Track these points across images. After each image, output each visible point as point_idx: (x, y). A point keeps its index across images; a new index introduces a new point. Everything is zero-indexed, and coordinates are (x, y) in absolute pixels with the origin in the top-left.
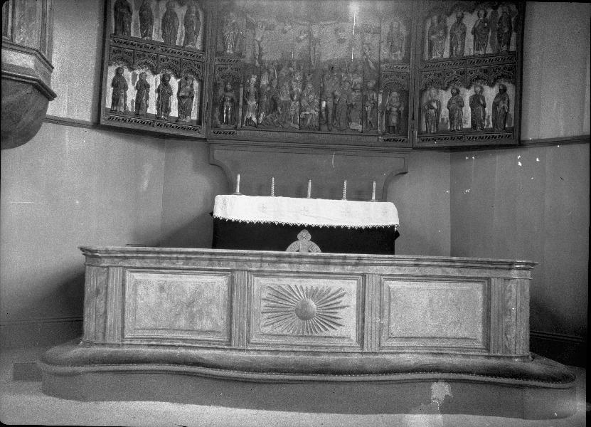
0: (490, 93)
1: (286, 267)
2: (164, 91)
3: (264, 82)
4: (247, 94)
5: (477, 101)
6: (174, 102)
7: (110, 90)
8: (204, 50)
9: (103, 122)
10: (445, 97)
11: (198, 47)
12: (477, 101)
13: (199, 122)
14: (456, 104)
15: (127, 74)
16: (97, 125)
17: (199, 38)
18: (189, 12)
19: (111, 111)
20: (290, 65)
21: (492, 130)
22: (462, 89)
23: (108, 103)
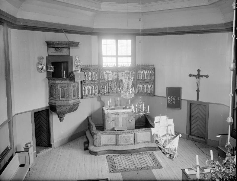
0: (149, 86)
1: (124, 133)
3: (109, 85)
4: (106, 87)
5: (147, 88)
12: (147, 88)
14: (143, 87)
18: (95, 73)
20: (114, 81)
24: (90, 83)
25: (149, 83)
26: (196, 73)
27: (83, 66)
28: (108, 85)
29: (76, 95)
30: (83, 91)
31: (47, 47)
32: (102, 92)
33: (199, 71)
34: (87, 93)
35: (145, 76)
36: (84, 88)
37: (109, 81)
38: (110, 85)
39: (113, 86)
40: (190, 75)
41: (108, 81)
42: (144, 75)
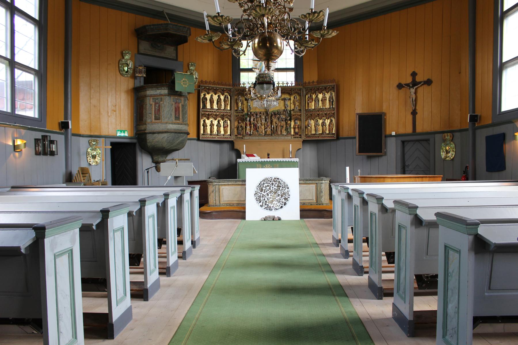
0: (328, 122)
2: (219, 126)
3: (252, 120)
5: (323, 124)
6: (222, 129)
7: (202, 127)
8: (231, 110)
10: (312, 122)
11: (229, 109)
12: (323, 124)
13: (230, 135)
14: (316, 125)
15: (207, 121)
16: (198, 139)
17: (229, 106)
18: (225, 97)
19: (203, 135)
20: (260, 113)
21: (328, 134)
22: (319, 120)
23: (202, 132)
24: (215, 114)
25: (328, 116)
26: (409, 80)
27: (202, 81)
28: (250, 121)
29: (181, 117)
30: (202, 127)
32: (238, 133)
33: (414, 74)
34: (209, 131)
35: (320, 102)
36: (204, 121)
37: (251, 113)
38: (254, 120)
39: (259, 122)
40: (400, 86)
41: (250, 115)
42: (319, 101)
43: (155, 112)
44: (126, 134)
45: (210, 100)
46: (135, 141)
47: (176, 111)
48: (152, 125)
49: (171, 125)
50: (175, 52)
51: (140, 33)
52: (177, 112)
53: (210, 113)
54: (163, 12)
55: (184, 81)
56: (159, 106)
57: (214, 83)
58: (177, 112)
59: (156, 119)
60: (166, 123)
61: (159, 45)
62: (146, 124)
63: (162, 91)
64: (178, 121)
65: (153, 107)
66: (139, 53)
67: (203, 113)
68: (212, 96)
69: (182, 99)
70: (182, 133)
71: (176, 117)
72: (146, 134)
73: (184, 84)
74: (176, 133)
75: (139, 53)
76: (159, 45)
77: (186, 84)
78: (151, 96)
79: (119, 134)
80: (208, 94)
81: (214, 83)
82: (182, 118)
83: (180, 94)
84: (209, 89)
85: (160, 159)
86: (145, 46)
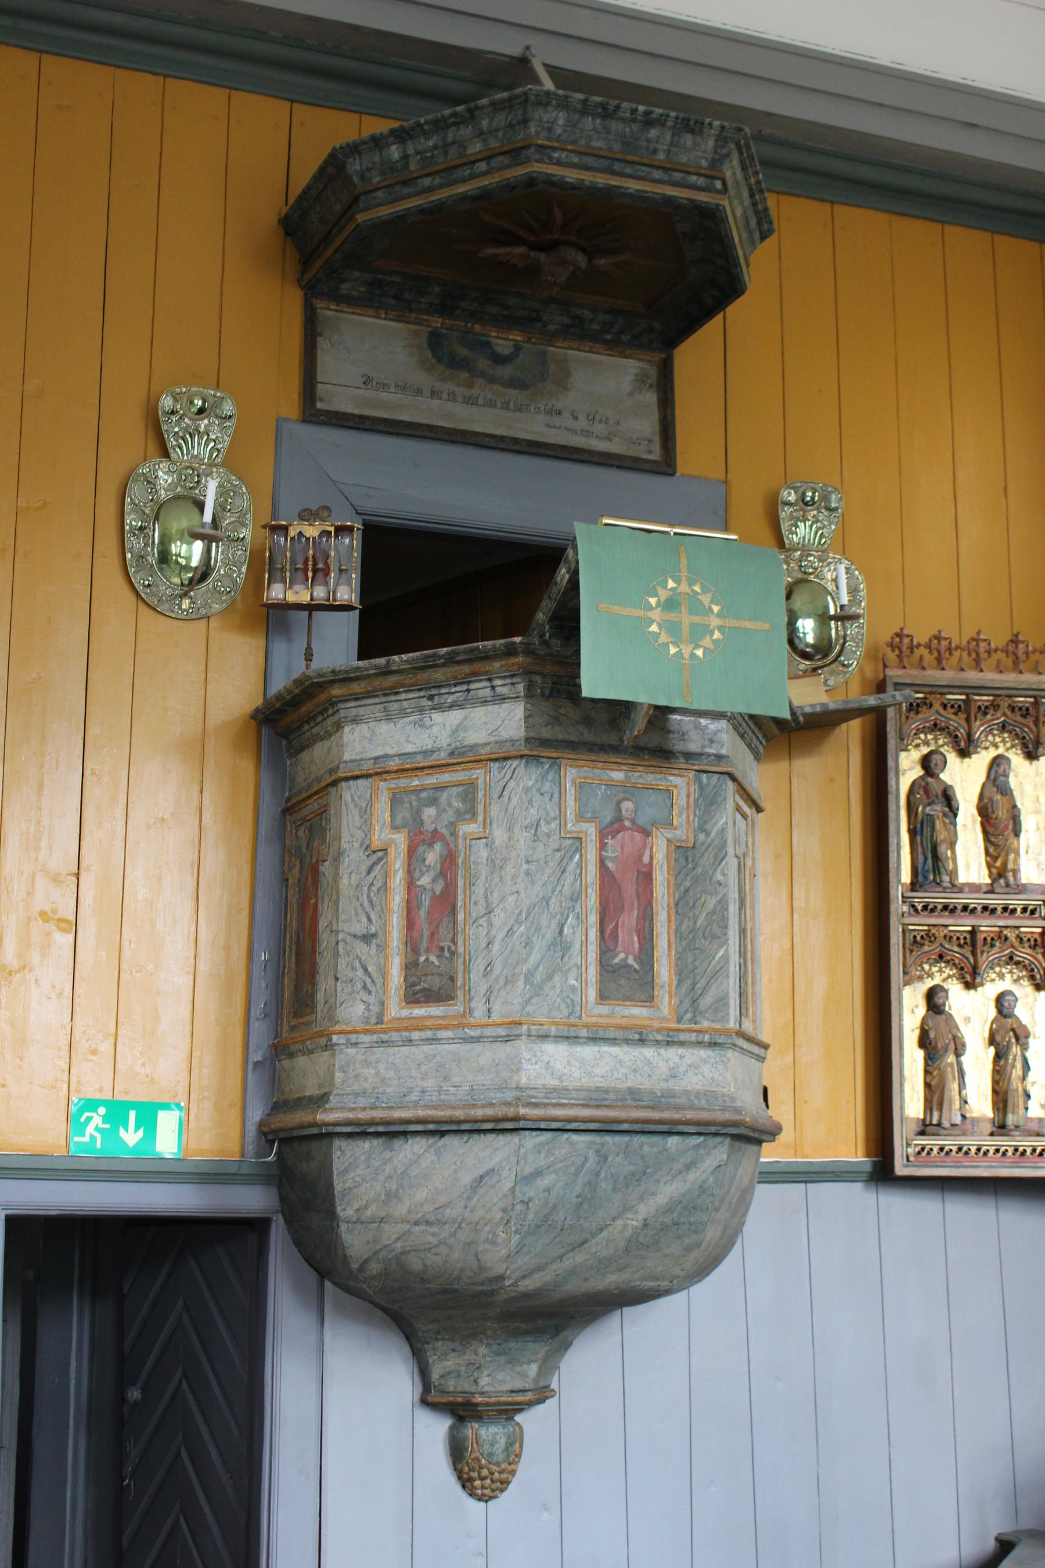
9: (900, 1169)
16: (882, 1171)
19: (925, 1129)
23: (911, 1101)
27: (901, 645)
29: (664, 970)
30: (911, 1062)
31: (295, 298)
34: (980, 1102)
36: (934, 1000)
43: (410, 923)
44: (167, 1142)
45: (985, 810)
46: (250, 1200)
47: (607, 912)
48: (377, 1060)
49: (556, 1053)
50: (651, 398)
51: (333, 249)
52: (629, 920)
53: (987, 926)
54: (523, 61)
55: (670, 604)
56: (449, 860)
57: (1015, 653)
58: (629, 920)
59: (415, 995)
60: (511, 1031)
61: (503, 345)
62: (329, 1047)
63: (478, 714)
64: (638, 1012)
65: (398, 880)
66: (313, 412)
67: (919, 923)
68: (997, 769)
69: (681, 785)
70: (670, 1129)
71: (608, 971)
72: (326, 1135)
73: (673, 629)
74: (607, 1128)
75: (313, 412)
76: (503, 345)
77: (698, 633)
78: (378, 771)
79: (91, 1137)
80: (964, 753)
81: (1015, 653)
82: (684, 972)
83: (636, 735)
84: (964, 709)
85: (494, 1380)
86: (373, 355)
